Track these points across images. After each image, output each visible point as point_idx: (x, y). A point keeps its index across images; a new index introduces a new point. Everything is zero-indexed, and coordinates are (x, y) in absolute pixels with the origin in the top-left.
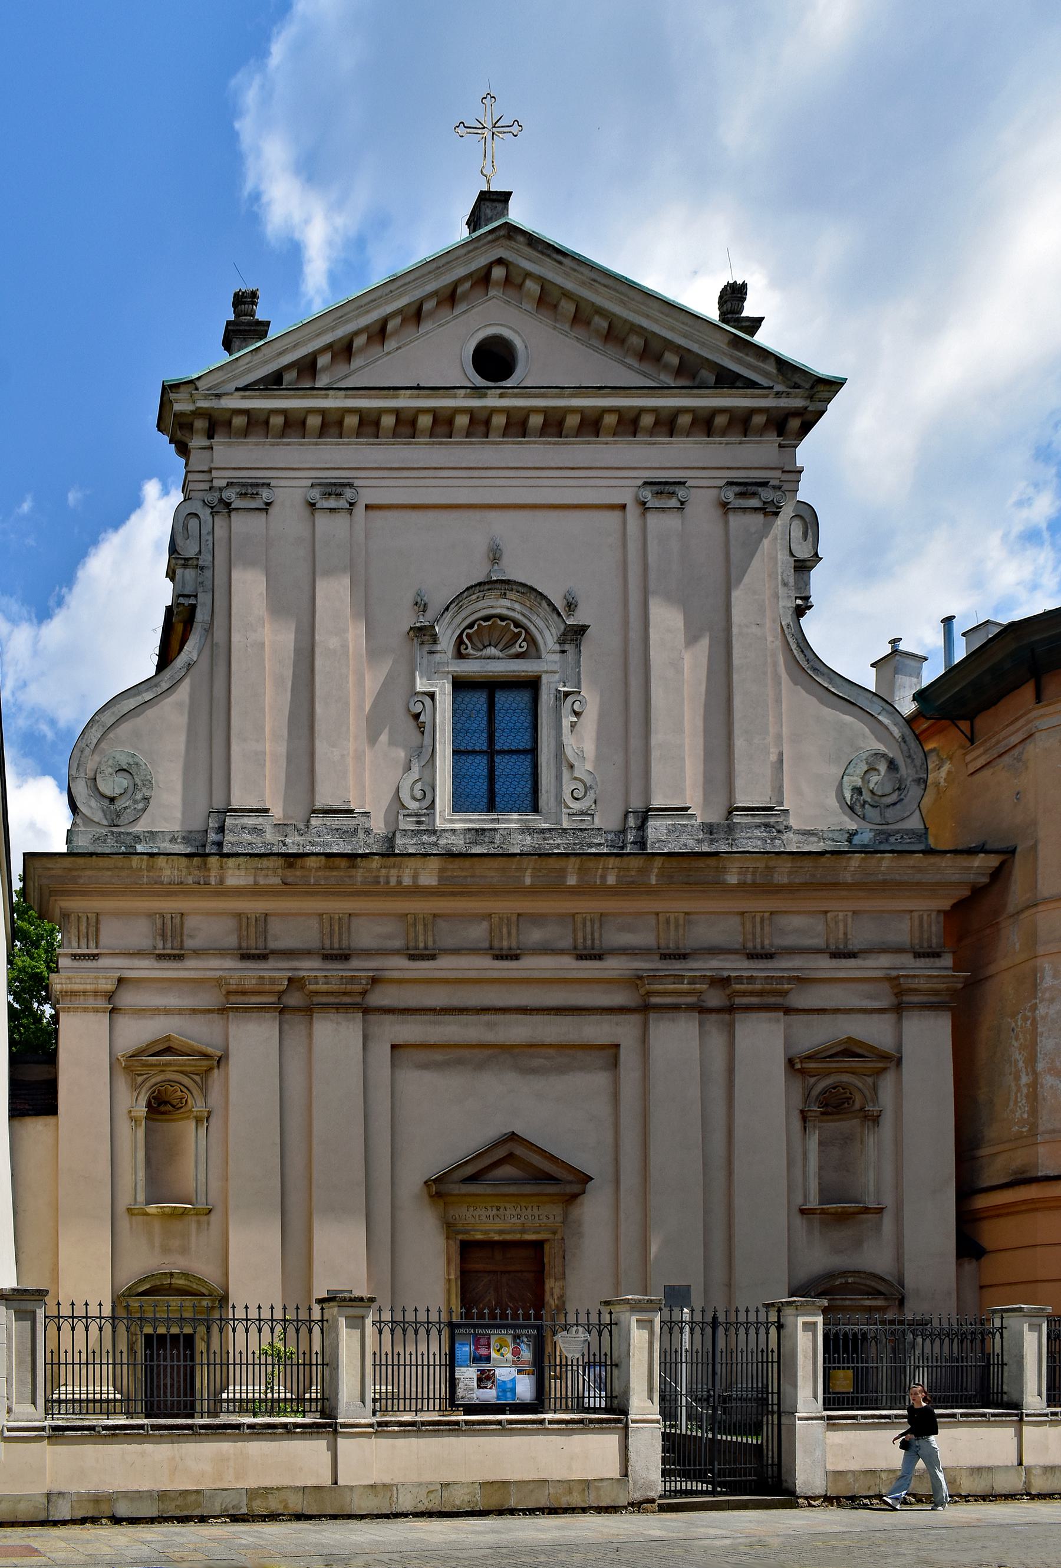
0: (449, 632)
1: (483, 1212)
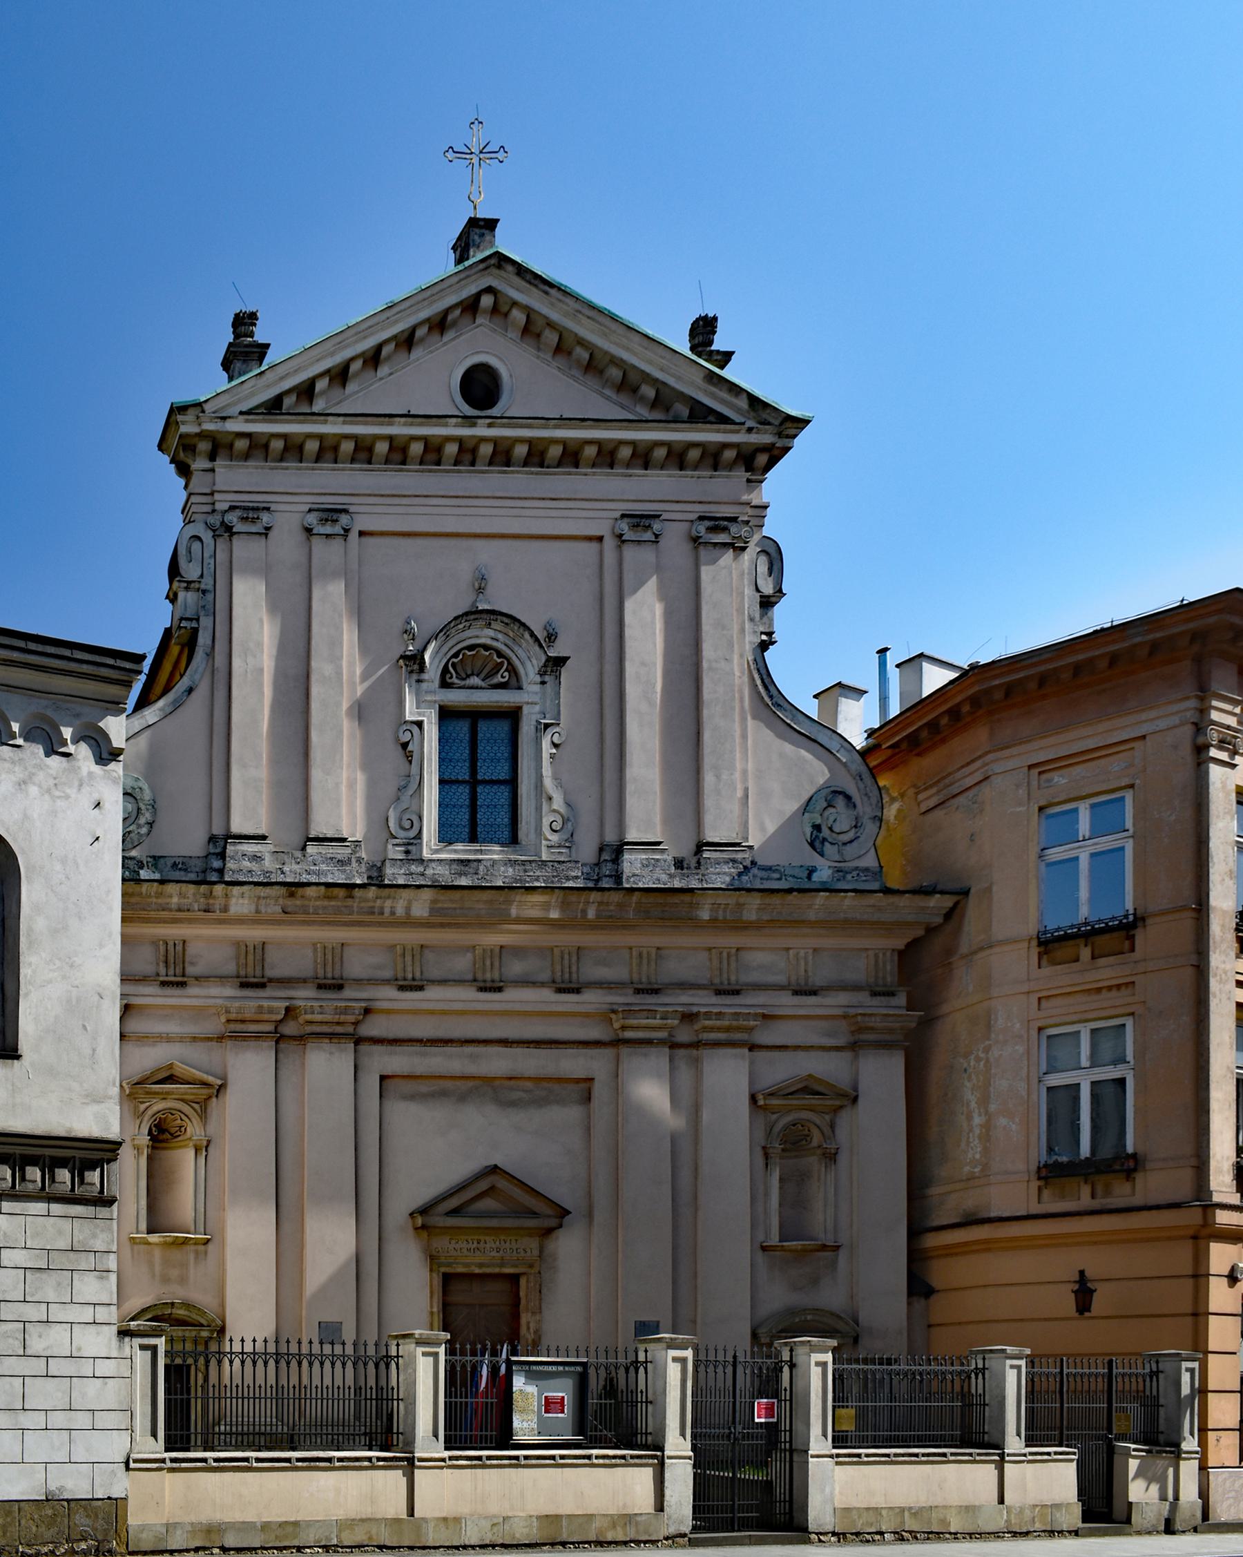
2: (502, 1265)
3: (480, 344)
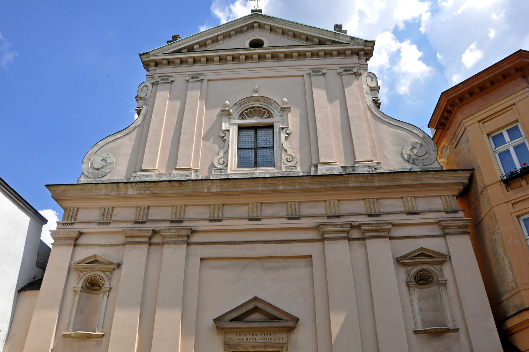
1: (245, 337)
2: (266, 347)
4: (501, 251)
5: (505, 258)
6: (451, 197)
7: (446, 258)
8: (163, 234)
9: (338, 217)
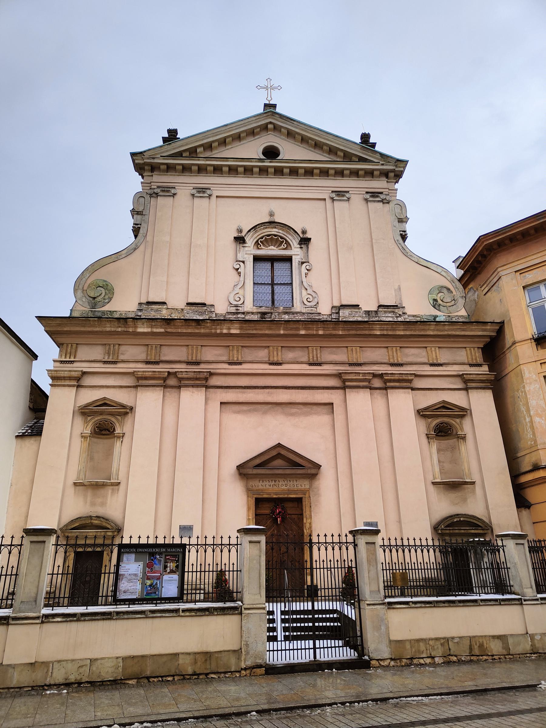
0: (252, 240)
1: (267, 483)
3: (270, 139)
4: (523, 409)
5: (527, 417)
6: (476, 349)
7: (466, 412)
8: (180, 376)
9: (360, 365)
